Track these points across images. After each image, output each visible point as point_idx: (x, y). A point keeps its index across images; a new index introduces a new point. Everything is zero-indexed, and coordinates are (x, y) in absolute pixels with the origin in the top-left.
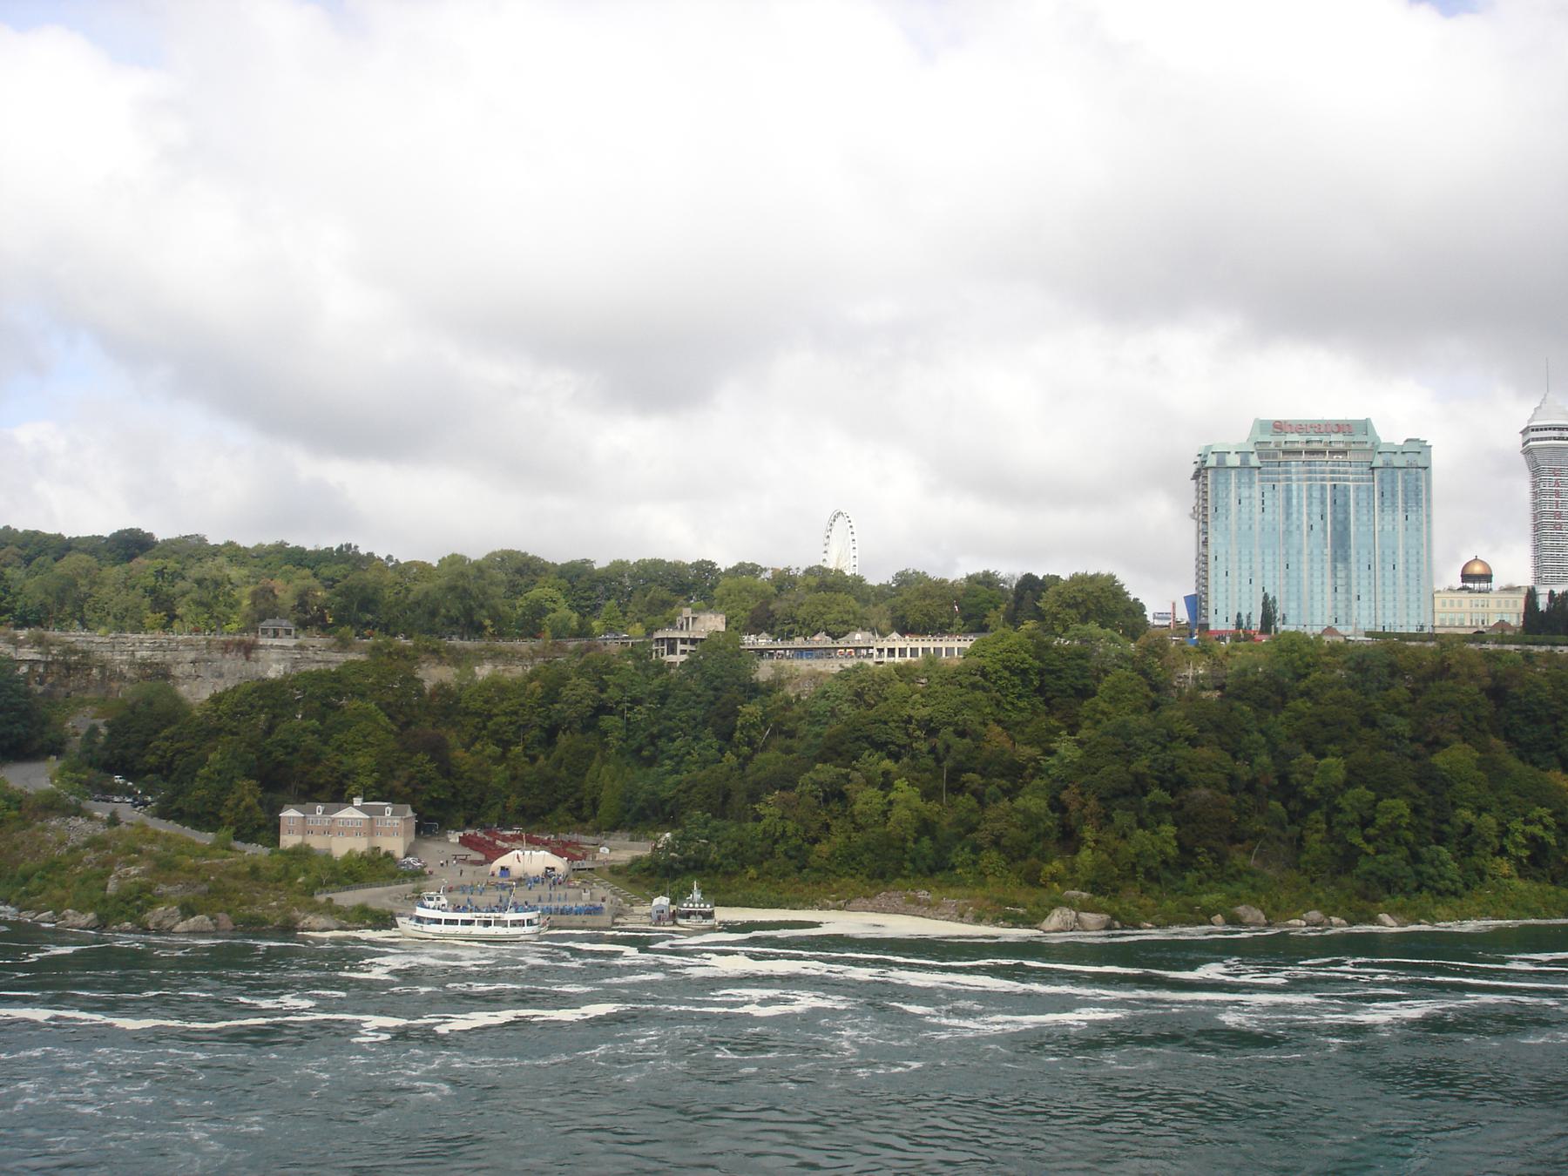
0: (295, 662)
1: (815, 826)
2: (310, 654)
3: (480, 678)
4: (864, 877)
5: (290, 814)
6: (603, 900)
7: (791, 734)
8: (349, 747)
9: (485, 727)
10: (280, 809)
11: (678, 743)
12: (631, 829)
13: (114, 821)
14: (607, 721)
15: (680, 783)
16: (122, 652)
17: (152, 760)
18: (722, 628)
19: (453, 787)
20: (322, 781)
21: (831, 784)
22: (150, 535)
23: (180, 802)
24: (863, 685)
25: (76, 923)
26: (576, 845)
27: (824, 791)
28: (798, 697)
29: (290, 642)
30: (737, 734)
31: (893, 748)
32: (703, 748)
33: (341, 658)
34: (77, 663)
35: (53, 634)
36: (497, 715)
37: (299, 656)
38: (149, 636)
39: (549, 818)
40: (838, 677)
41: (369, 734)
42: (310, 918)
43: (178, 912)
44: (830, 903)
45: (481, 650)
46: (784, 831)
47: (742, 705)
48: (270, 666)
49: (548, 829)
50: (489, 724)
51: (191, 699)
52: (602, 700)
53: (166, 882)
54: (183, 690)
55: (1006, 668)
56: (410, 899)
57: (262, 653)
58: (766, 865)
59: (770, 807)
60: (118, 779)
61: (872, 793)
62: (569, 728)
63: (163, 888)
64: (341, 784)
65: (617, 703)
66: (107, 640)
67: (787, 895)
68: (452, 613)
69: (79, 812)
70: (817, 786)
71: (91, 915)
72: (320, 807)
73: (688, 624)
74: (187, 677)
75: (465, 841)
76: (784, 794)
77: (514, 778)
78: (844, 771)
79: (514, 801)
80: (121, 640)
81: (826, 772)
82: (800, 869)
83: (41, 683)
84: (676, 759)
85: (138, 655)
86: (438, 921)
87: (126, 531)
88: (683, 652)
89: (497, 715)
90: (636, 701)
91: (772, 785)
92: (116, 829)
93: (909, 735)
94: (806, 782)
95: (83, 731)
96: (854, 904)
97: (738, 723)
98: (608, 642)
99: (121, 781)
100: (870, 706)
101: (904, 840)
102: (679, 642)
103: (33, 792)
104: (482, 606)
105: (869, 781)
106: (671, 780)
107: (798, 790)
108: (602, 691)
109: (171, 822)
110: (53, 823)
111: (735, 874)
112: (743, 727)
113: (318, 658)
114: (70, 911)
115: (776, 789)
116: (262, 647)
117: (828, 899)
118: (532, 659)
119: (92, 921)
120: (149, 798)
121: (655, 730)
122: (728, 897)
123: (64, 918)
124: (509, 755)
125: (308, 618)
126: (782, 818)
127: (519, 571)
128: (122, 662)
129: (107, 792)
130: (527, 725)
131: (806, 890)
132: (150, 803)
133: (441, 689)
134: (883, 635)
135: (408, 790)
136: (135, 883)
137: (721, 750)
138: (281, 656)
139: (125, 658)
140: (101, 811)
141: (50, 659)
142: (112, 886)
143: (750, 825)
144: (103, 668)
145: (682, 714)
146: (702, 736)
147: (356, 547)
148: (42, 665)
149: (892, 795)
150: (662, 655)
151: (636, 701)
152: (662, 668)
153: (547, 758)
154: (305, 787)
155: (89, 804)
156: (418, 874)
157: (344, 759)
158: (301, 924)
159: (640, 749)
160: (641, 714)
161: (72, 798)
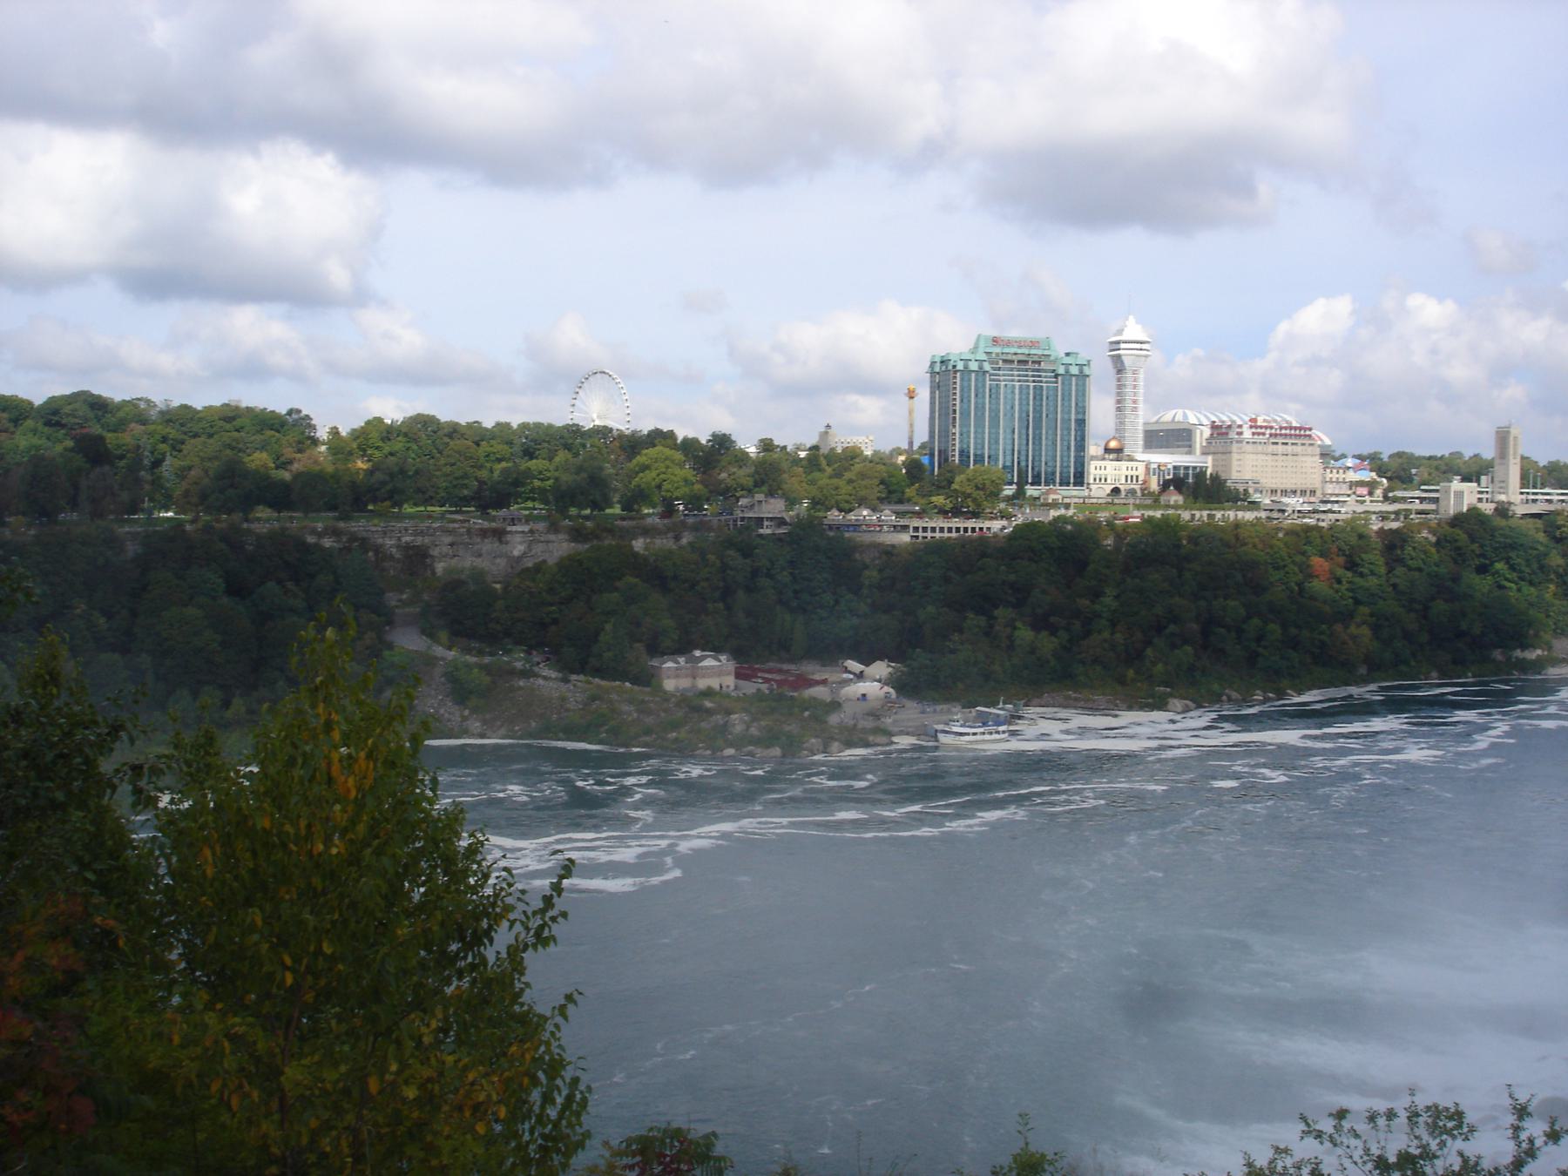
48: (514, 548)
57: (509, 537)
74: (444, 556)
86: (968, 734)
113: (542, 539)
116: (510, 532)
139: (392, 542)
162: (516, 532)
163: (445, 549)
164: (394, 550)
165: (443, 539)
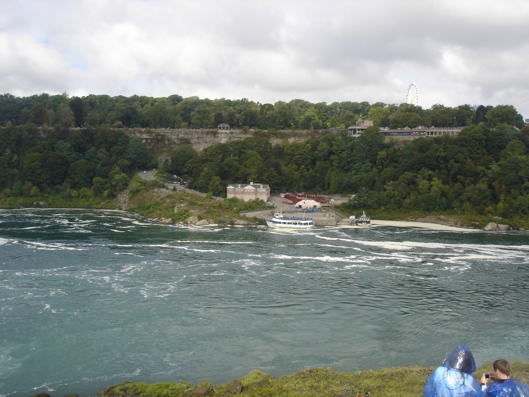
0: (230, 138)
1: (405, 193)
2: (235, 135)
3: (290, 143)
4: (421, 210)
5: (230, 187)
6: (333, 217)
7: (396, 162)
8: (249, 166)
9: (292, 159)
10: (227, 186)
11: (357, 164)
12: (341, 193)
13: (175, 189)
14: (333, 157)
15: (358, 178)
16: (175, 135)
17: (186, 170)
18: (372, 125)
19: (282, 179)
20: (240, 177)
21: (411, 179)
22: (181, 97)
23: (195, 184)
24: (422, 144)
25: (165, 222)
26: (323, 198)
27: (408, 181)
28: (399, 149)
29: (228, 131)
30: (377, 162)
31: (432, 166)
32: (366, 166)
33: (244, 136)
34: (161, 139)
35: (153, 130)
36: (296, 155)
37: (231, 136)
38: (183, 130)
39: (313, 189)
40: (413, 142)
41: (255, 161)
42: (238, 221)
43: (197, 218)
44: (410, 219)
45: (290, 133)
47: (379, 151)
48: (222, 140)
49: (314, 193)
50: (294, 158)
51: (197, 150)
52: (331, 150)
53: (193, 209)
54: (194, 147)
55: (474, 139)
56: (270, 215)
57: (219, 135)
58: (388, 206)
59: (389, 186)
60: (175, 176)
61: (425, 182)
62: (320, 159)
63: (192, 211)
64: (246, 178)
65: (336, 151)
66: (170, 132)
67: (395, 216)
68: (280, 121)
69: (164, 187)
70: (406, 179)
71: (170, 219)
72: (239, 185)
73: (360, 124)
75: (286, 197)
76: (394, 182)
77: (302, 176)
78: (415, 174)
79: (302, 184)
80: (174, 131)
81: (409, 175)
82: (399, 207)
83: (150, 146)
84: (356, 170)
85: (180, 136)
86: (280, 223)
87: (173, 95)
88: (359, 133)
89: (296, 155)
90: (342, 150)
91: (390, 179)
92: (175, 192)
93: (438, 162)
94: (401, 178)
95: (163, 161)
96: (419, 219)
97: (378, 158)
98: (333, 130)
99: (176, 177)
100: (424, 152)
101: (436, 198)
102: (357, 130)
103: (149, 181)
104: (290, 119)
105: (424, 178)
106: (354, 177)
107: (399, 181)
108: (331, 147)
109: (193, 190)
110: (156, 190)
111: (377, 208)
112: (379, 159)
113: (237, 136)
114: (163, 218)
115: (391, 180)
116: (219, 133)
118: (307, 136)
119: (171, 221)
120: (185, 182)
121: (349, 160)
122: (375, 216)
123: (161, 220)
124: (300, 168)
125: (233, 124)
126: (393, 190)
127: (302, 107)
128: (175, 139)
129: (172, 180)
131: (401, 215)
132: (185, 184)
133: (277, 147)
134: (429, 127)
135: (267, 180)
136: (183, 209)
137: (372, 167)
138: (225, 136)
139: (175, 137)
140: (171, 186)
141: (152, 138)
142: (176, 210)
143: (382, 193)
144: (169, 140)
145: (359, 155)
146: (365, 162)
147: (247, 99)
148: (150, 140)
149: (432, 183)
150: (351, 135)
151: (342, 150)
152: (351, 139)
153: (313, 169)
154: (234, 179)
155: (166, 184)
156: (272, 207)
157: (247, 170)
158: (236, 223)
159: (344, 166)
160: (344, 154)
161: (161, 182)
162: (222, 133)
163: (196, 140)
164: (176, 140)
165: (195, 136)
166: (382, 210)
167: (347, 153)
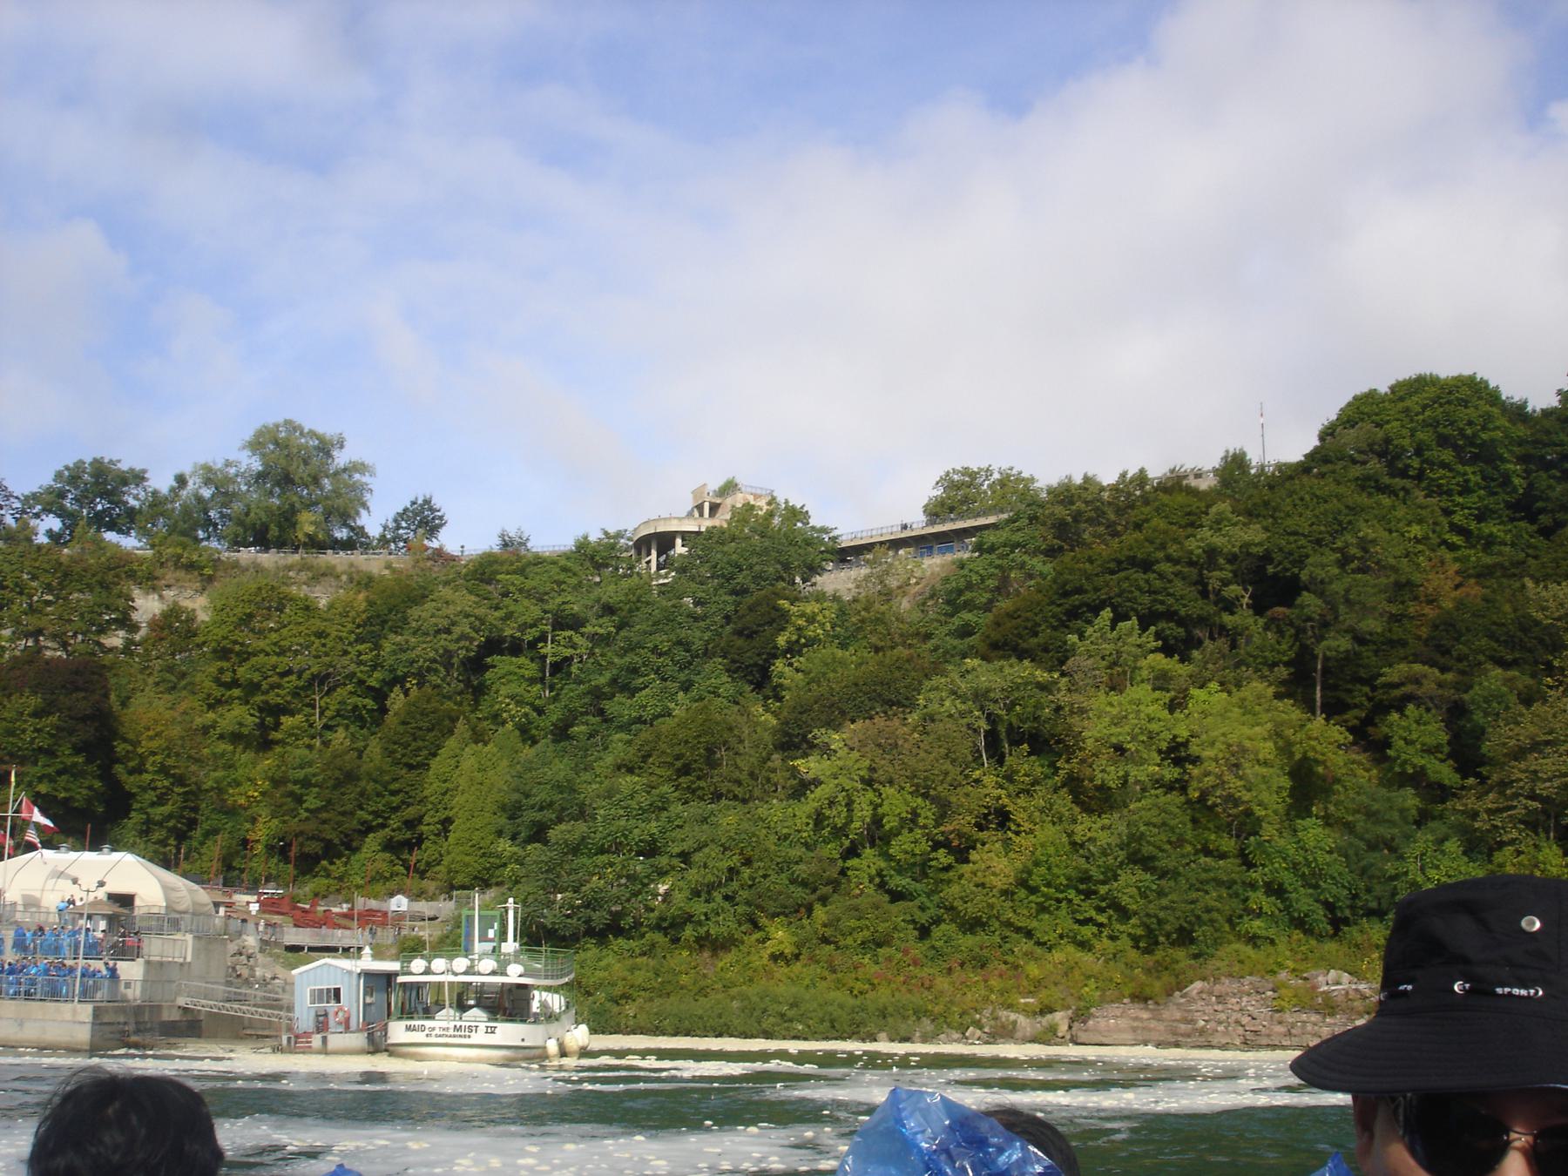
4: (1125, 943)
44: (1022, 1020)
45: (289, 568)
46: (877, 821)
55: (1443, 441)
67: (883, 995)
117: (1010, 1007)
126: (869, 782)
130: (328, 676)
131: (942, 983)
143: (776, 810)
151: (563, 622)
166: (775, 958)
167: (593, 638)
